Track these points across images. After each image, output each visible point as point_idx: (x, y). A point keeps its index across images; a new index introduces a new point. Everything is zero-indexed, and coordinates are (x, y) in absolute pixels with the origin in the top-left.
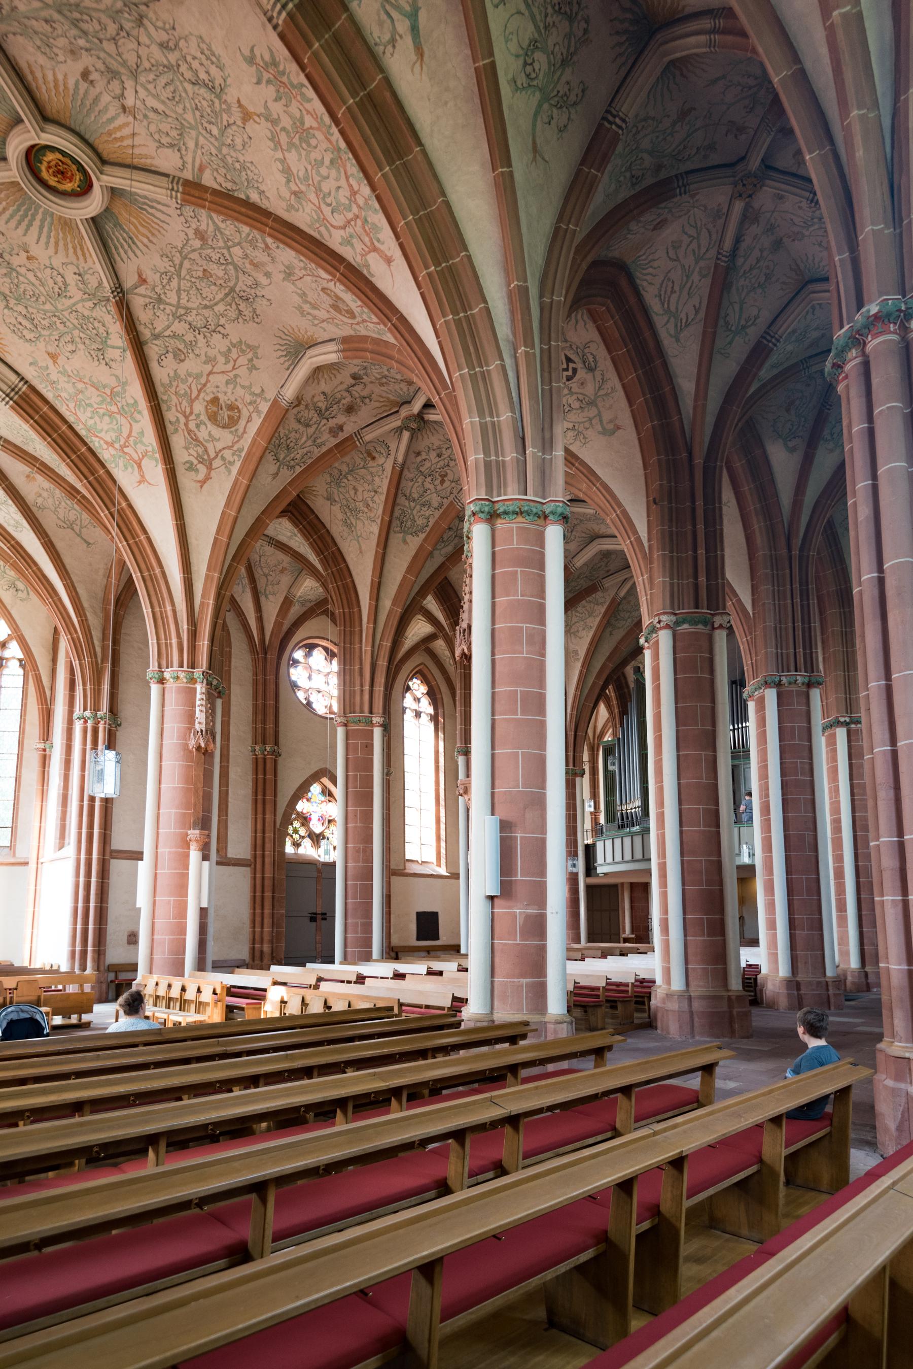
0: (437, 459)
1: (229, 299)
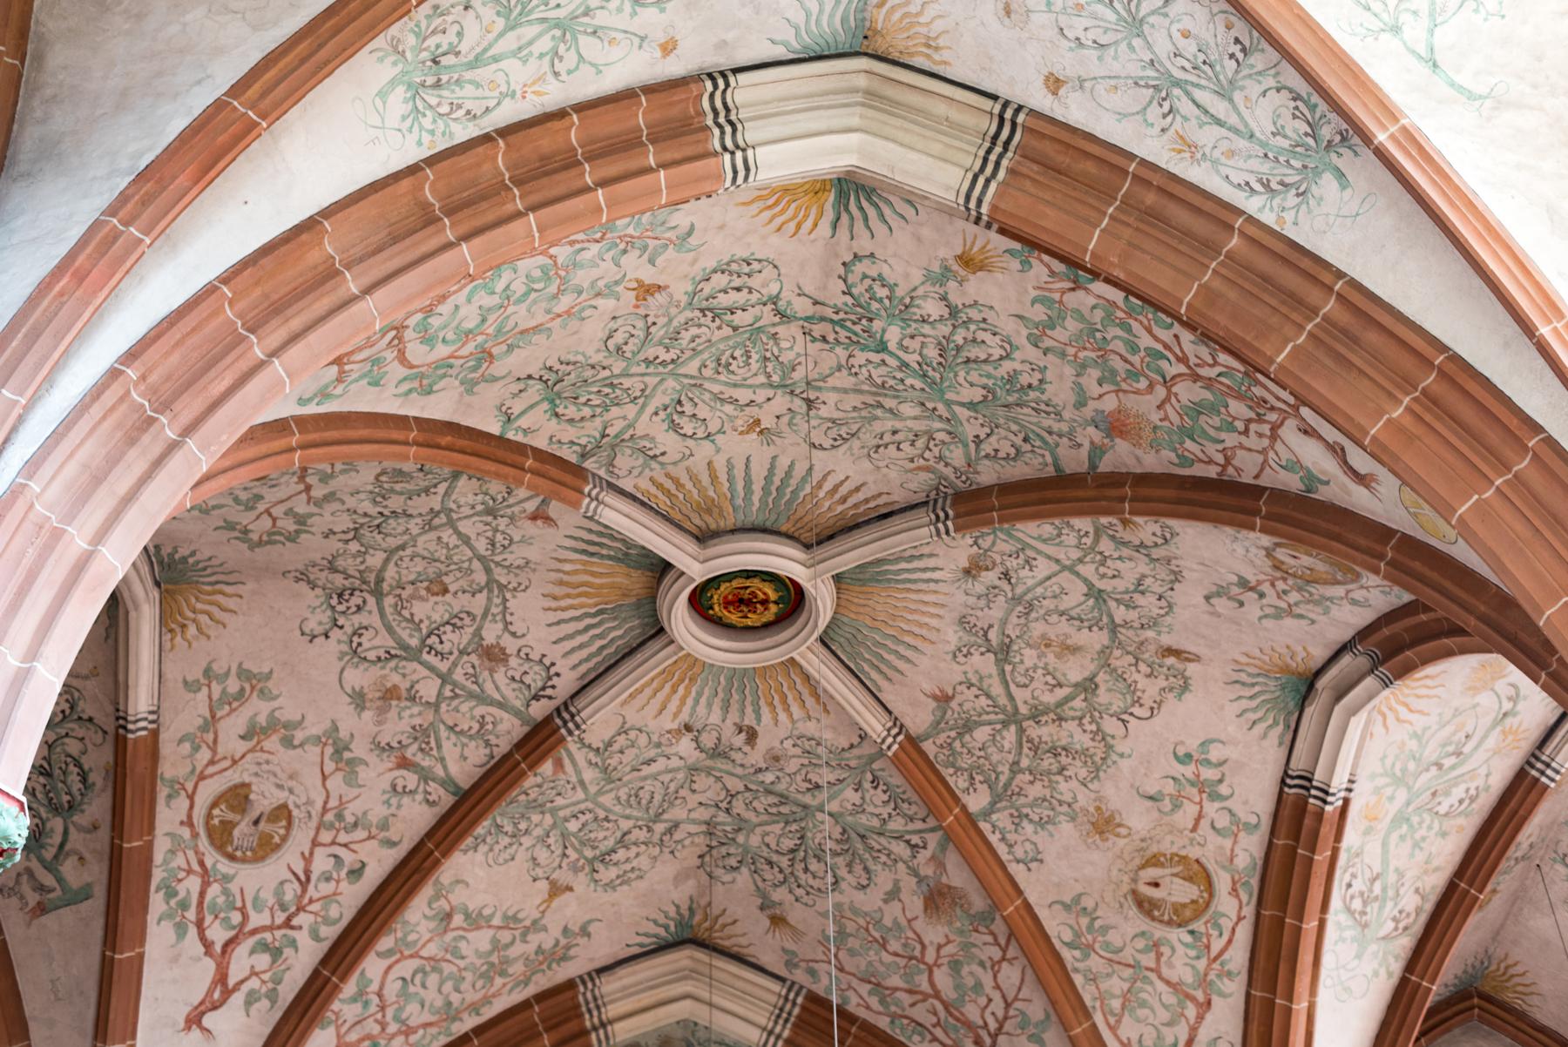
1: (372, 577)
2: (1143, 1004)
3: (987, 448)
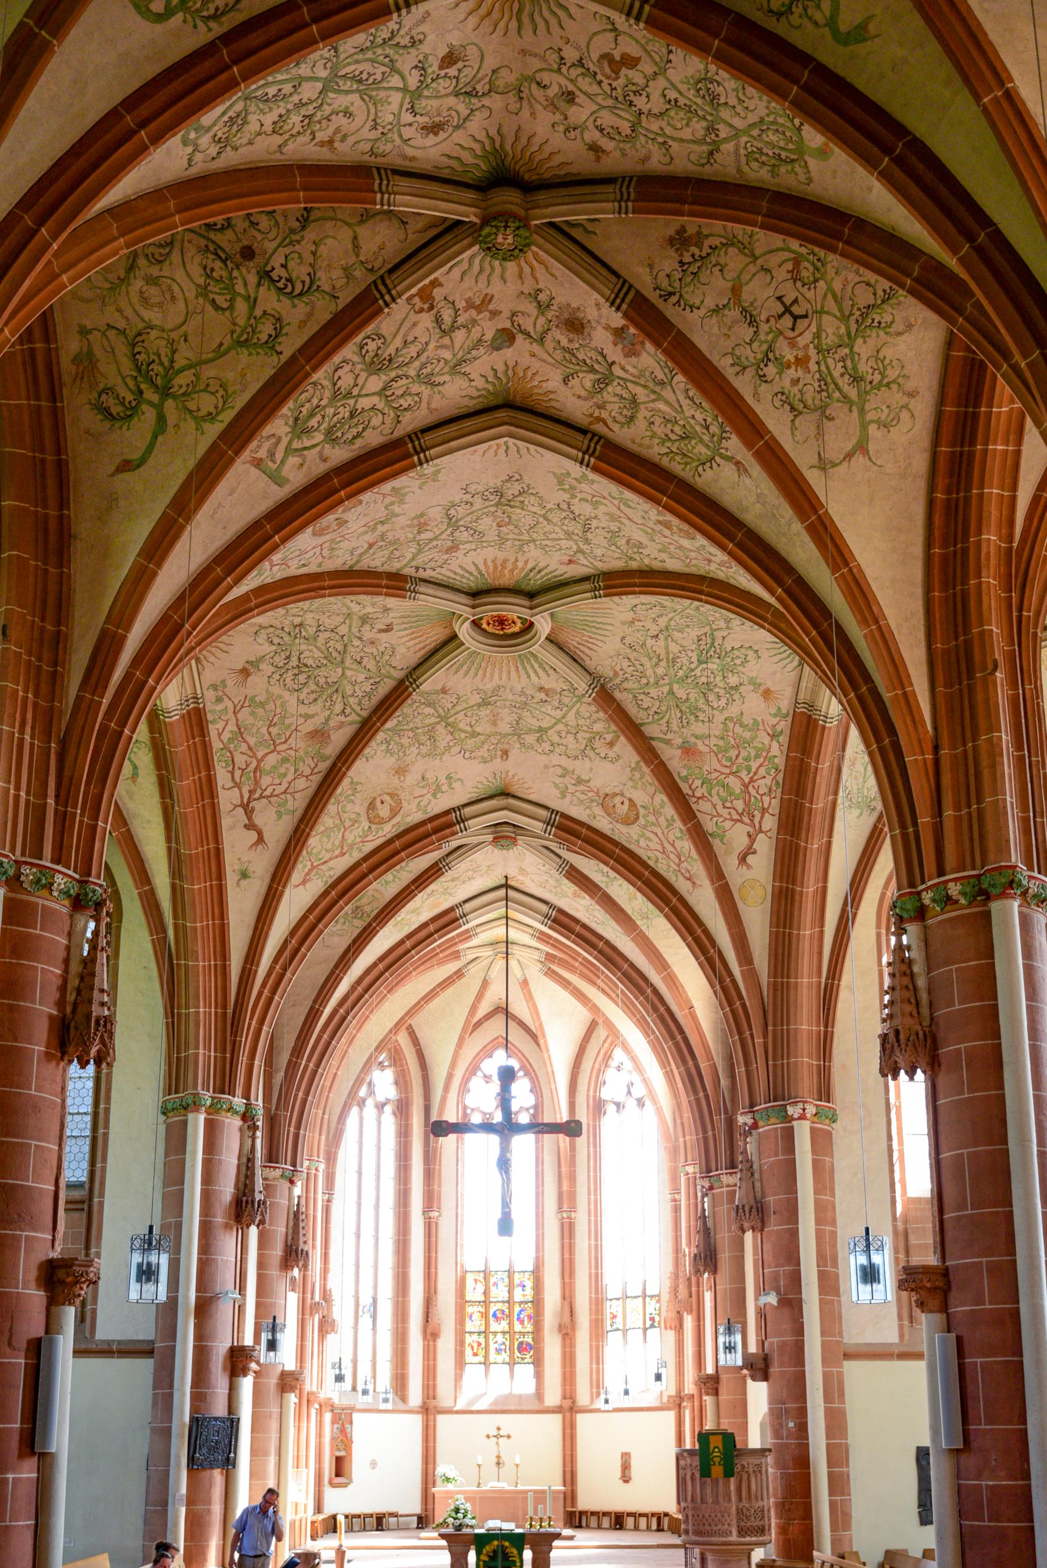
0: (581, 99)
2: (329, 838)
3: (642, 697)
